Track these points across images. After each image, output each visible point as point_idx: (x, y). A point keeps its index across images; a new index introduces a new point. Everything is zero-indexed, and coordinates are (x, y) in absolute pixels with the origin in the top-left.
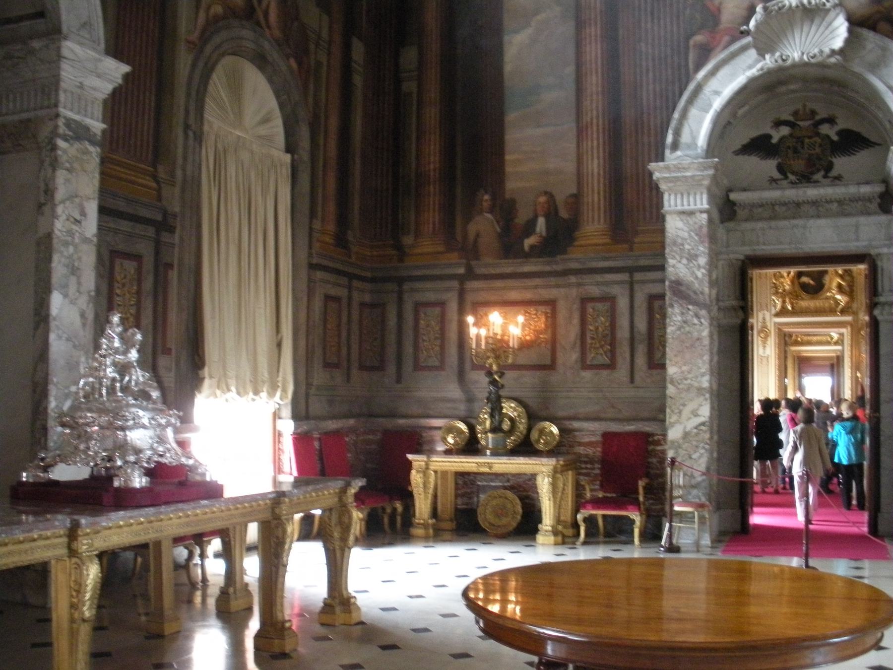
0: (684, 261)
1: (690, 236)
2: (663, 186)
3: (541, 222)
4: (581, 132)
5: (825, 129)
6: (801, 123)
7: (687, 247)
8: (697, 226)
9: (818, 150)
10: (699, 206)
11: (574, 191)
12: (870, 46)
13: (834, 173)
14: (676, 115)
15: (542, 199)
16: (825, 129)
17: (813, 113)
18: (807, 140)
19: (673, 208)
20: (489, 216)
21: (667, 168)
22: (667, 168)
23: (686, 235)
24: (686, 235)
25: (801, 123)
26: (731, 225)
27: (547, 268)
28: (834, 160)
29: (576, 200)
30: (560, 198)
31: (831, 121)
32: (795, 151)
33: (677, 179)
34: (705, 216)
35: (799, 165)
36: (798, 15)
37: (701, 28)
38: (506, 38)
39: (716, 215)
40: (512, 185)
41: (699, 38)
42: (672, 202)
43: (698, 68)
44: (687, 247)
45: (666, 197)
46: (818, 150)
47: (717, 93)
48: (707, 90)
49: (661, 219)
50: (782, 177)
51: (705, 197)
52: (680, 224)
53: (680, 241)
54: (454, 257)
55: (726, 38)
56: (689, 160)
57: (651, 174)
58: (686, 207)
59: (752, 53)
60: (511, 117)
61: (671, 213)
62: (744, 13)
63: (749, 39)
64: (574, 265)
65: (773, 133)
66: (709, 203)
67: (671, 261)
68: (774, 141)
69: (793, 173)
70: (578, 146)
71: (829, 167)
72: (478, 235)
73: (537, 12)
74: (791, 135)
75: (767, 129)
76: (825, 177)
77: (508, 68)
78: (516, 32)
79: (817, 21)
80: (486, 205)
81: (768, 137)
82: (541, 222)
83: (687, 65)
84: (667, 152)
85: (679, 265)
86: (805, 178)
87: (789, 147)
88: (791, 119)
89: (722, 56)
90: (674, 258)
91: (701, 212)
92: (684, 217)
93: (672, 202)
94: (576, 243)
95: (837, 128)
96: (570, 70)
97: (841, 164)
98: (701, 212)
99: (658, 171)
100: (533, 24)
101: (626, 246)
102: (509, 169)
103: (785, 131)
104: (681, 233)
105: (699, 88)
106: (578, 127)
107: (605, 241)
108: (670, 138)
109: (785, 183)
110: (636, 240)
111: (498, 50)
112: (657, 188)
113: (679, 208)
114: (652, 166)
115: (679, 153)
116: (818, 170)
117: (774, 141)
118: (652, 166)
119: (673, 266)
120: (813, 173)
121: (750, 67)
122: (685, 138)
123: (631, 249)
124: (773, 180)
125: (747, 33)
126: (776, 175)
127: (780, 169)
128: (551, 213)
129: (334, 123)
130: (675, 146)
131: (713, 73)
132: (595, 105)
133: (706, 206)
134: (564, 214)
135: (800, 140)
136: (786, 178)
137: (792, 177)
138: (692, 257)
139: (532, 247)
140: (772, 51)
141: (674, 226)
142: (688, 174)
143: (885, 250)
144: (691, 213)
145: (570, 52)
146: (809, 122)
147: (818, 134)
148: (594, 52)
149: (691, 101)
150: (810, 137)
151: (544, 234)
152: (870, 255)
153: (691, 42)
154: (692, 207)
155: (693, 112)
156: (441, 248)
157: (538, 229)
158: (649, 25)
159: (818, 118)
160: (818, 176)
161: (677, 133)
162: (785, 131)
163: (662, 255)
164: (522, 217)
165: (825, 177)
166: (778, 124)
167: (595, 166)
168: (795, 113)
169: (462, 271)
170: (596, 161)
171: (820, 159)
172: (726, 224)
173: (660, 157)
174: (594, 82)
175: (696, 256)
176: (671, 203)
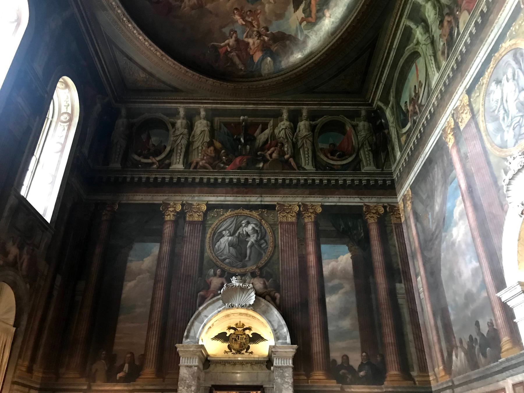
0: (186, 388)
1: (189, 377)
2: (180, 354)
3: (127, 365)
4: (150, 327)
7: (187, 382)
8: (192, 373)
9: (244, 341)
10: (194, 364)
11: (143, 353)
12: (263, 304)
13: (250, 351)
14: (189, 324)
15: (129, 355)
16: (247, 332)
17: (243, 325)
18: (240, 336)
19: (183, 364)
20: (103, 361)
21: (183, 346)
22: (183, 346)
23: (187, 376)
24: (187, 376)
26: (207, 370)
27: (126, 388)
29: (143, 357)
30: (136, 356)
31: (249, 329)
32: (235, 340)
33: (187, 351)
34: (196, 368)
35: (237, 346)
36: (239, 290)
37: (203, 289)
38: (125, 283)
39: (201, 367)
40: (117, 348)
41: (201, 293)
42: (183, 361)
43: (200, 306)
44: (187, 382)
45: (181, 358)
46: (244, 341)
47: (206, 316)
48: (203, 315)
49: (178, 368)
51: (197, 360)
52: (185, 371)
53: (184, 379)
54: (83, 380)
55: (212, 295)
56: (192, 344)
57: (176, 348)
58: (189, 364)
59: (221, 301)
60: (121, 317)
61: (183, 366)
62: (220, 285)
63: (220, 296)
64: (138, 387)
65: (227, 332)
66: (198, 363)
67: (180, 388)
68: (228, 335)
69: (234, 349)
70: (147, 333)
71: (248, 348)
72: (97, 370)
73: (139, 274)
74: (234, 333)
76: (246, 352)
77: (123, 296)
78: (130, 281)
79: (245, 292)
80: (103, 356)
81: (226, 333)
82: (127, 365)
83: (196, 303)
84: (184, 339)
85: (183, 390)
86: (239, 352)
88: (235, 326)
89: (209, 302)
90: (181, 386)
91: (195, 366)
92: (188, 368)
93: (183, 361)
94: (141, 377)
95: (252, 332)
96: (149, 300)
98: (195, 366)
99: (179, 347)
100: (137, 279)
101: (162, 379)
102: (116, 340)
103: (232, 331)
104: (185, 375)
105: (200, 313)
106: (149, 324)
107: (154, 377)
108: (185, 334)
109: (230, 353)
110: (167, 377)
111: (121, 288)
112: (178, 354)
113: (186, 364)
114: (177, 345)
115: (188, 340)
116: (244, 349)
117: (228, 335)
118: (177, 345)
119: (181, 390)
120: (242, 350)
121: (220, 307)
122: (192, 334)
123: (164, 381)
124: (226, 352)
125: (219, 295)
126: (228, 350)
127: (229, 347)
128: (132, 363)
129: (39, 313)
130: (187, 337)
131: (205, 308)
132: (157, 316)
133: (197, 364)
134: (137, 363)
135: (238, 336)
136: (231, 351)
138: (189, 386)
139: (120, 377)
140: (228, 302)
141: (183, 372)
142: (191, 350)
143: (268, 386)
144: (191, 367)
145: (150, 293)
147: (245, 334)
148: (160, 294)
149: (195, 319)
150: (241, 335)
151: (127, 372)
152: (262, 387)
153: (199, 294)
154: (191, 364)
155: (196, 323)
156: (78, 376)
157: (124, 369)
158: (183, 286)
159: (245, 327)
160: (244, 351)
161: (189, 332)
162: (232, 331)
163: (177, 384)
164: (118, 364)
165: (246, 352)
166: (230, 328)
167: (154, 342)
168: (237, 324)
169: (85, 387)
170: (154, 340)
171: (244, 344)
172: (205, 371)
173: (181, 342)
174: (158, 306)
175: (190, 386)
176: (183, 362)
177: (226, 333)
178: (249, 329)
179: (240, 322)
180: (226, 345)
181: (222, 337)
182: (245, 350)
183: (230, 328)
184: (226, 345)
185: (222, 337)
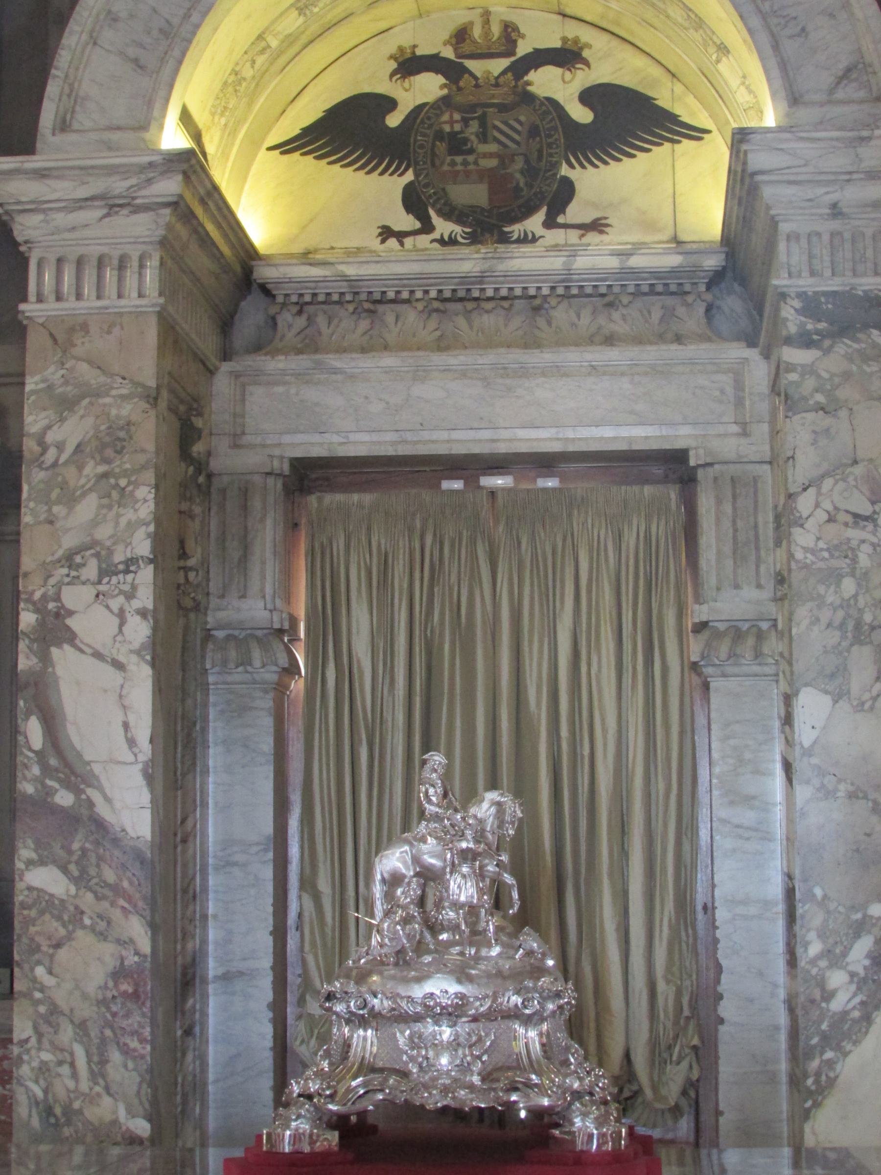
5: (546, 82)
6: (475, 66)
13: (575, 213)
17: (510, 34)
25: (475, 66)
28: (574, 174)
31: (567, 56)
50: (418, 225)
69: (450, 213)
74: (445, 102)
75: (383, 86)
76: (550, 223)
86: (489, 225)
87: (439, 135)
88: (448, 53)
95: (582, 79)
97: (596, 183)
103: (429, 87)
109: (423, 240)
126: (406, 222)
127: (413, 201)
136: (427, 227)
137: (443, 227)
146: (503, 63)
147: (528, 98)
159: (523, 49)
160: (535, 223)
162: (429, 87)
165: (550, 223)
166: (409, 65)
168: (461, 36)
177: (389, 104)
178: (567, 56)
179: (486, 15)
180: (394, 185)
181: (349, 132)
182: (540, 216)
183: (409, 65)
184: (394, 185)
185: (349, 132)
